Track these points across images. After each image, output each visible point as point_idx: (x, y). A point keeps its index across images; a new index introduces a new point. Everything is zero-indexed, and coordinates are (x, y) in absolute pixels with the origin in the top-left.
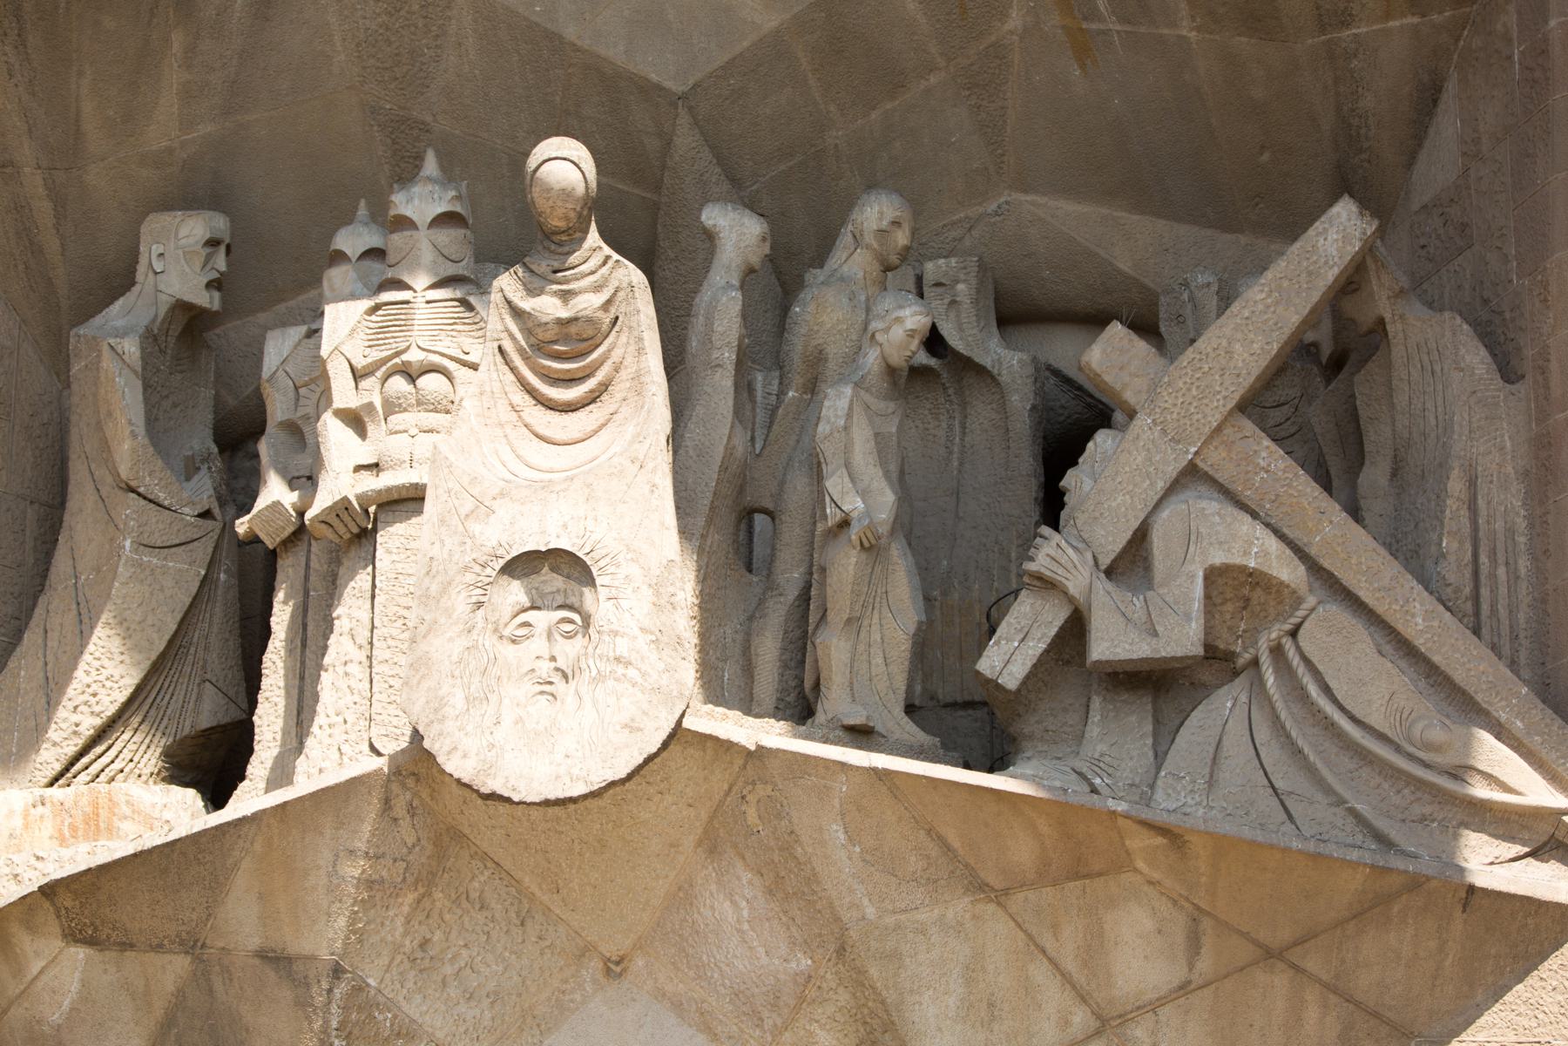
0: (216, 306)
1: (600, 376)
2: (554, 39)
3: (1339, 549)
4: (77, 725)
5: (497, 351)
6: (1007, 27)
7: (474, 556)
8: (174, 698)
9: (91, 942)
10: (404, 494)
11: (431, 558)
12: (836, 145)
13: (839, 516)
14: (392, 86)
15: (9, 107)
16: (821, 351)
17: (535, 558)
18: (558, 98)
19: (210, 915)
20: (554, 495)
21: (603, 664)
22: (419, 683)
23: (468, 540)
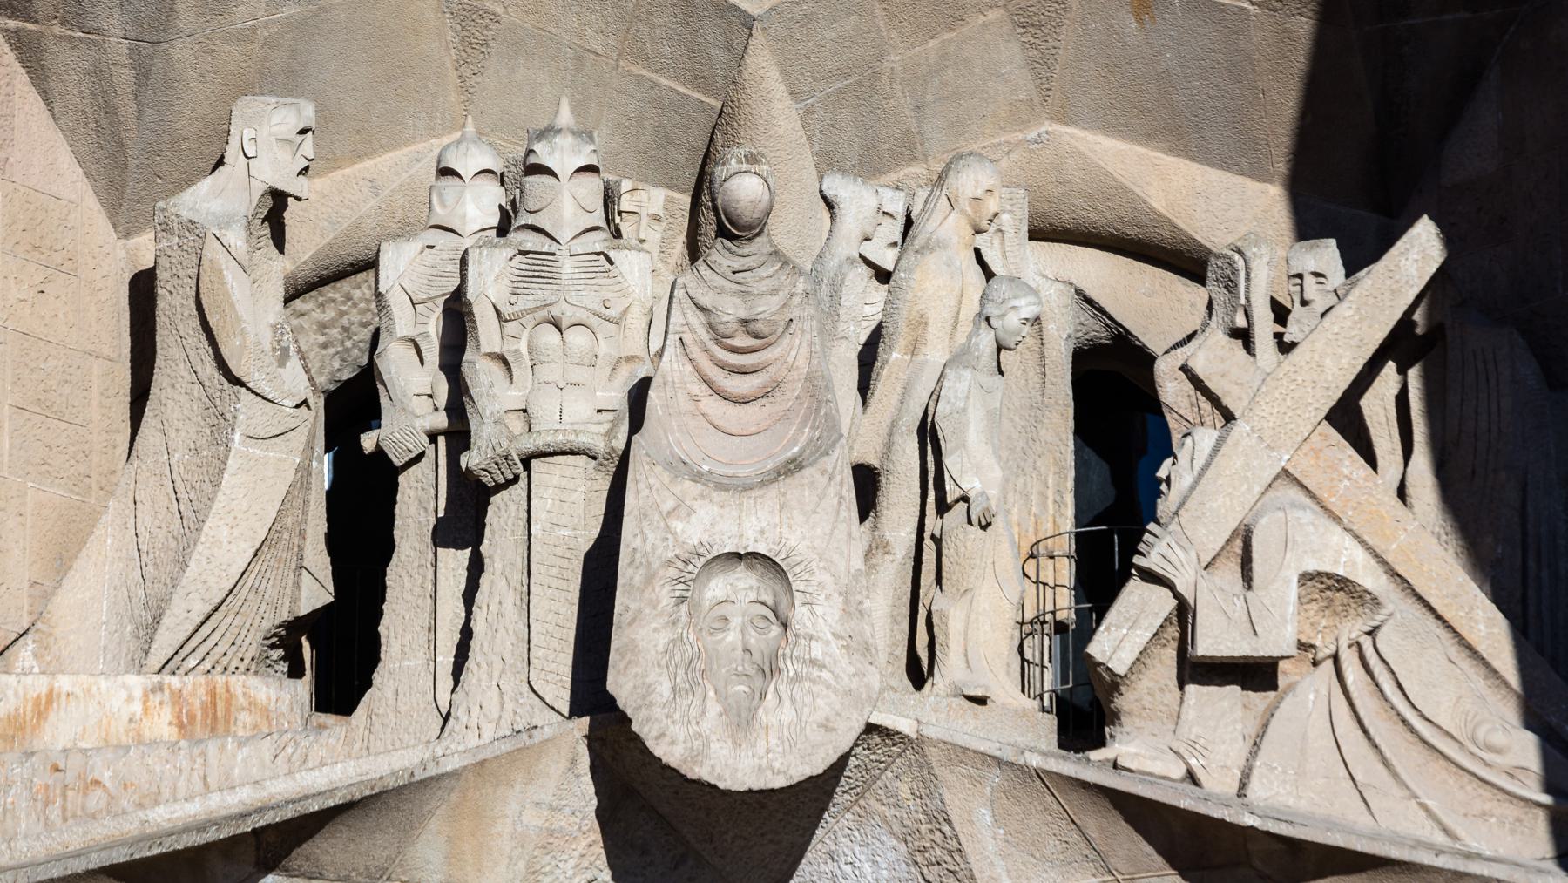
7: (677, 552)
12: (892, 69)
13: (958, 493)
19: (400, 853)
22: (626, 668)
23: (669, 536)
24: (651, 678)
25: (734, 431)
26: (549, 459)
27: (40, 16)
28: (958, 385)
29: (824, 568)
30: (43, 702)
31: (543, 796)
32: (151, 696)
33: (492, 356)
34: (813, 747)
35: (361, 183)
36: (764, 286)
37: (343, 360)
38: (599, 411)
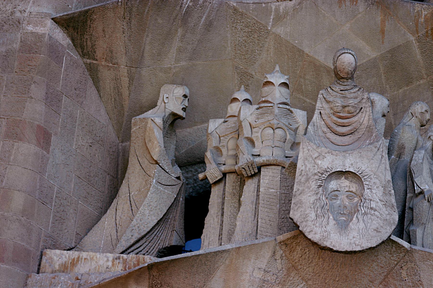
0: (184, 116)
2: (301, 52)
4: (132, 236)
5: (319, 113)
7: (319, 170)
8: (163, 235)
10: (272, 163)
14: (244, 61)
15: (120, 44)
16: (403, 145)
17: (340, 174)
18: (298, 72)
19: (205, 285)
20: (348, 155)
21: (367, 209)
22: (297, 209)
23: (316, 165)
24: (307, 212)
25: (339, 144)
26: (268, 167)
27: (98, 58)
28: (419, 155)
29: (376, 178)
30: (76, 260)
31: (262, 265)
32: (115, 260)
33: (247, 138)
34: (372, 237)
35: (203, 130)
36: (352, 95)
37: (193, 189)
38: (287, 157)
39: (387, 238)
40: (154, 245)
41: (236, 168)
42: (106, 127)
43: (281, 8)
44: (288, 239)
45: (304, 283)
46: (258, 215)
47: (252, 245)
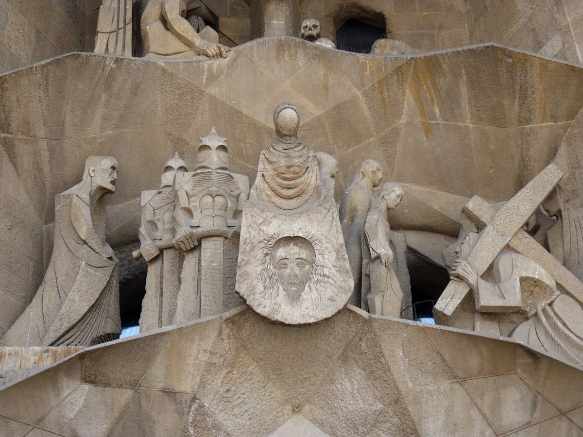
0: (113, 190)
1: (301, 186)
2: (239, 114)
3: (563, 278)
4: (61, 325)
5: (262, 175)
6: (400, 122)
7: (264, 237)
9: (93, 382)
10: (213, 234)
11: (246, 238)
13: (376, 255)
16: (355, 208)
17: (288, 240)
18: (237, 135)
19: (145, 373)
22: (243, 281)
23: (262, 233)
26: (209, 239)
29: (327, 242)
32: (44, 354)
36: (297, 154)
38: (229, 227)
39: (343, 307)
40: (87, 335)
41: (174, 241)
42: (26, 207)
43: (215, 67)
44: (235, 315)
45: (255, 364)
46: (201, 293)
47: (194, 325)
